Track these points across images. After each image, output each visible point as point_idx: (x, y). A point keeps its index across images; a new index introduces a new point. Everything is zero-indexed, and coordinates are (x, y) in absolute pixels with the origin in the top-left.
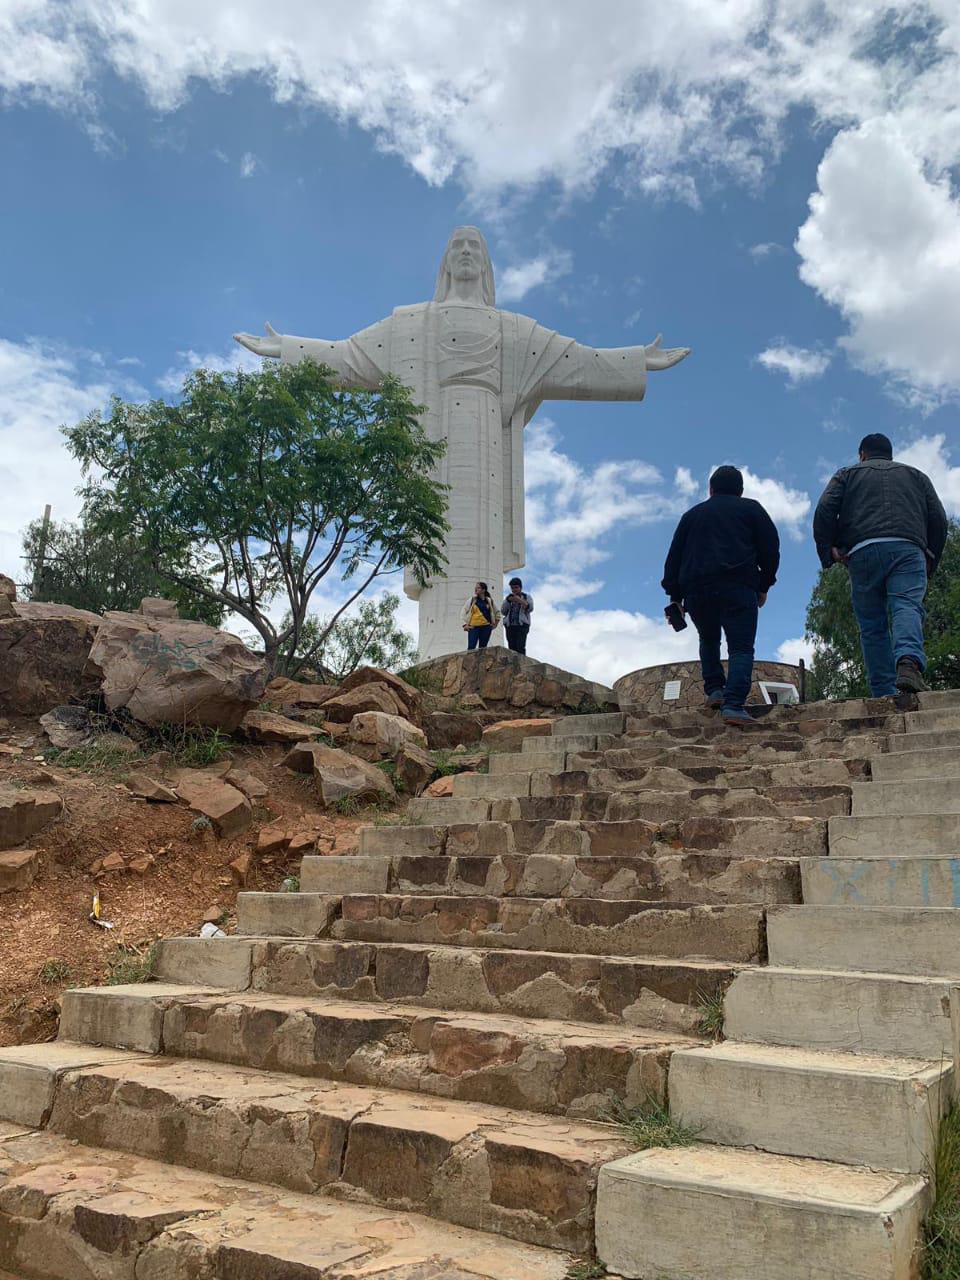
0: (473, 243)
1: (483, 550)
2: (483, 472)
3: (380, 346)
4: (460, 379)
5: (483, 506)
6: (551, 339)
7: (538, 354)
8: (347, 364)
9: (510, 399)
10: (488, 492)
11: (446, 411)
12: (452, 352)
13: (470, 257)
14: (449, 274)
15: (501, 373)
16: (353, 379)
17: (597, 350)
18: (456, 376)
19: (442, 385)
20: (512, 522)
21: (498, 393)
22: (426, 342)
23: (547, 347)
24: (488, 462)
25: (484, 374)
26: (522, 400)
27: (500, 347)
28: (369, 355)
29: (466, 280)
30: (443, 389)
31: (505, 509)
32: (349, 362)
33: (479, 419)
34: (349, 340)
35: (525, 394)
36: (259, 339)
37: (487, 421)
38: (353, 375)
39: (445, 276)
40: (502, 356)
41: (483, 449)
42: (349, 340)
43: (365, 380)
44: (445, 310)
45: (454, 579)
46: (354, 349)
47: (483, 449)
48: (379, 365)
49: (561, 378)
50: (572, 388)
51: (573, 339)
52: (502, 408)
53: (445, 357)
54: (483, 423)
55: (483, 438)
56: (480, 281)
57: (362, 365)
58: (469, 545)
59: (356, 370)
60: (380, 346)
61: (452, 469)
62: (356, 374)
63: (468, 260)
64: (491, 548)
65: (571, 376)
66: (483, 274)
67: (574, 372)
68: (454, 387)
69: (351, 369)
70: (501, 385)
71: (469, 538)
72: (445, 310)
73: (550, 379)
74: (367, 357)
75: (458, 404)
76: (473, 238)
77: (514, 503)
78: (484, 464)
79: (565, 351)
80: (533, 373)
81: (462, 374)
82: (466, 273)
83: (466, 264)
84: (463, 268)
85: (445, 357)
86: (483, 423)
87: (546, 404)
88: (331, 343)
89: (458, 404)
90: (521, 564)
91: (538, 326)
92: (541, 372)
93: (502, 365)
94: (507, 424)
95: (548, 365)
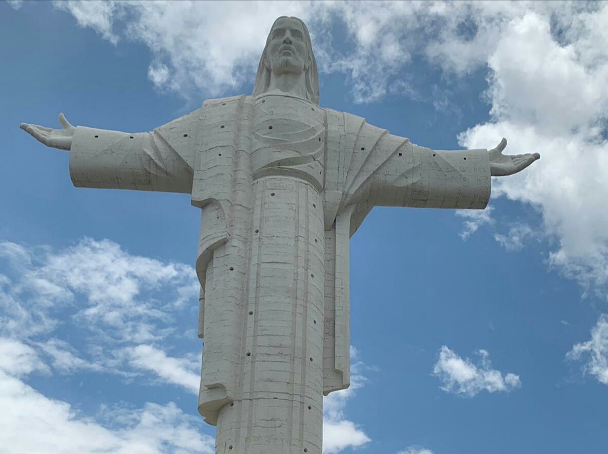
0: (295, 33)
2: (301, 270)
3: (186, 136)
4: (278, 168)
5: (300, 310)
6: (381, 137)
7: (368, 149)
8: (145, 153)
9: (334, 196)
10: (307, 293)
11: (258, 203)
12: (267, 141)
13: (292, 46)
14: (269, 71)
15: (325, 168)
17: (435, 151)
18: (272, 164)
19: (255, 177)
20: (334, 336)
21: (321, 189)
22: (239, 130)
23: (377, 143)
24: (307, 261)
25: (306, 165)
26: (348, 199)
27: (324, 139)
28: (173, 146)
29: (287, 73)
30: (256, 181)
31: (326, 321)
32: (150, 153)
33: (297, 212)
34: (152, 133)
35: (352, 192)
36: (50, 131)
37: (307, 216)
39: (265, 73)
40: (326, 150)
41: (302, 245)
42: (152, 133)
44: (262, 100)
45: (260, 395)
46: (156, 140)
47: (302, 245)
48: (182, 154)
49: (392, 176)
50: (407, 188)
51: (406, 139)
52: (324, 207)
53: (260, 145)
54: (302, 217)
55: (302, 233)
56: (303, 74)
57: (163, 155)
58: (280, 354)
59: (156, 161)
60: (186, 136)
61: (263, 266)
62: (156, 164)
63: (290, 49)
64: (308, 359)
65: (404, 175)
66: (306, 71)
67: (408, 172)
68: (268, 178)
69: (150, 159)
70: (324, 182)
71: (280, 346)
72: (262, 100)
73: (381, 177)
74: (170, 147)
75: (273, 195)
76: (295, 28)
77: (337, 313)
78: (302, 263)
79: (398, 149)
80: (361, 170)
81: (279, 163)
82: (287, 63)
83: (289, 54)
84: (284, 58)
85: (260, 145)
86: (302, 217)
87: (377, 211)
88: (129, 134)
89: (273, 195)
90: (345, 383)
91: (366, 124)
92: (372, 168)
93: (325, 160)
94: (331, 227)
95: (380, 162)
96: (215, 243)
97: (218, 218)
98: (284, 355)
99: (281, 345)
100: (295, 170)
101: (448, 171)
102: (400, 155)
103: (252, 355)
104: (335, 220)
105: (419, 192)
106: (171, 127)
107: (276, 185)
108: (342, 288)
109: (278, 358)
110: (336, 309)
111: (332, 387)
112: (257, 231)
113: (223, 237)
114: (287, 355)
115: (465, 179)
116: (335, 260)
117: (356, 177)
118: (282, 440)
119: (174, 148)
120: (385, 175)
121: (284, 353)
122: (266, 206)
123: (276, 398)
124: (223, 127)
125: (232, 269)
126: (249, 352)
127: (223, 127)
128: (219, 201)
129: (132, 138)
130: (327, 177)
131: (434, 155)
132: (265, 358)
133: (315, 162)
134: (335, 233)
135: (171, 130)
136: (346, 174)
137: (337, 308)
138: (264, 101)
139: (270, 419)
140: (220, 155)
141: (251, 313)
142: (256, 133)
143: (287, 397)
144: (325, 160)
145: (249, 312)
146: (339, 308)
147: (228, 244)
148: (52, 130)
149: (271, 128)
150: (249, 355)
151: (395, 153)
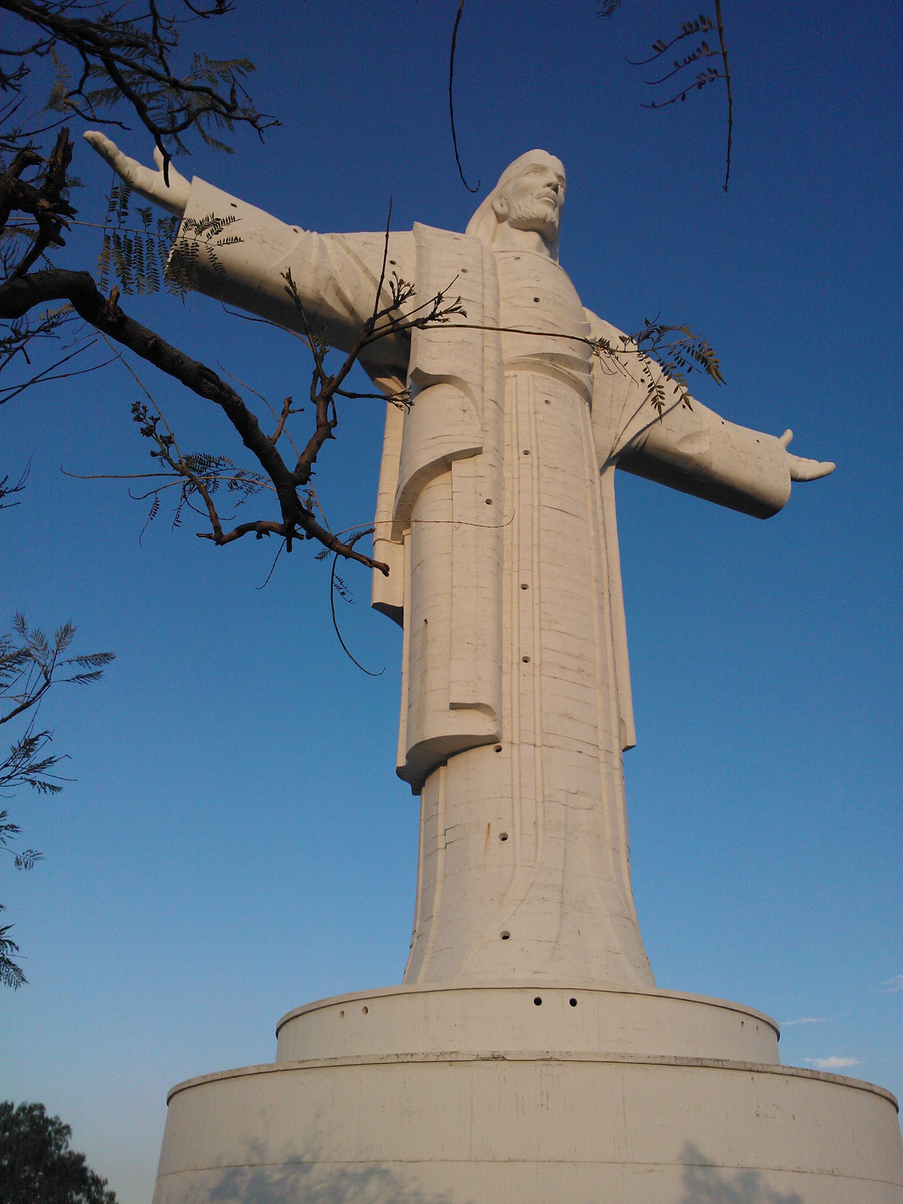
16: (331, 300)
18: (542, 355)
43: (352, 311)
65: (690, 438)
89: (547, 402)
97: (464, 411)
99: (582, 655)
100: (574, 376)
101: (741, 452)
115: (761, 469)
118: (598, 836)
122: (540, 417)
123: (581, 752)
125: (488, 502)
128: (469, 385)
133: (589, 375)
139: (574, 792)
145: (521, 583)
147: (479, 458)
149: (536, 300)
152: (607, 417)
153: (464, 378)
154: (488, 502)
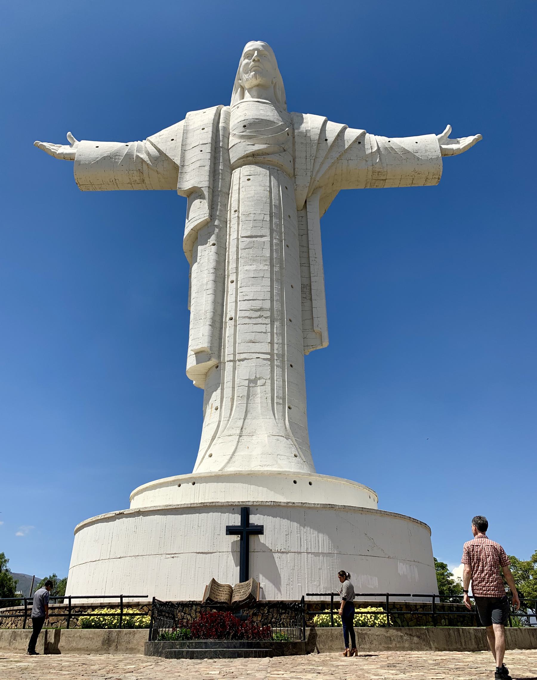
1: (277, 324)
3: (173, 140)
18: (247, 156)
20: (311, 299)
31: (303, 286)
38: (145, 167)
45: (243, 356)
58: (260, 317)
60: (173, 140)
75: (249, 180)
77: (313, 279)
79: (358, 138)
80: (326, 158)
81: (253, 155)
89: (249, 180)
96: (198, 224)
98: (265, 318)
102: (359, 143)
103: (235, 319)
104: (306, 202)
105: (379, 172)
106: (161, 135)
107: (251, 172)
108: (315, 258)
109: (260, 320)
110: (311, 276)
111: (312, 346)
112: (235, 211)
113: (206, 218)
114: (266, 318)
116: (308, 234)
117: (322, 163)
119: (162, 150)
120: (348, 160)
121: (264, 316)
124: (203, 129)
126: (232, 316)
127: (203, 129)
129: (127, 146)
130: (296, 165)
131: (389, 142)
132: (247, 321)
134: (307, 212)
135: (160, 137)
136: (313, 161)
137: (312, 275)
138: (238, 107)
140: (201, 151)
141: (232, 282)
142: (233, 132)
143: (269, 357)
144: (294, 151)
146: (314, 275)
148: (61, 146)
150: (231, 319)
151: (355, 141)
152: (304, 169)
153: (200, 186)
154: (214, 245)
